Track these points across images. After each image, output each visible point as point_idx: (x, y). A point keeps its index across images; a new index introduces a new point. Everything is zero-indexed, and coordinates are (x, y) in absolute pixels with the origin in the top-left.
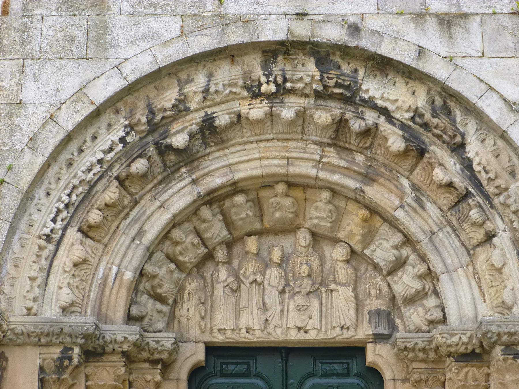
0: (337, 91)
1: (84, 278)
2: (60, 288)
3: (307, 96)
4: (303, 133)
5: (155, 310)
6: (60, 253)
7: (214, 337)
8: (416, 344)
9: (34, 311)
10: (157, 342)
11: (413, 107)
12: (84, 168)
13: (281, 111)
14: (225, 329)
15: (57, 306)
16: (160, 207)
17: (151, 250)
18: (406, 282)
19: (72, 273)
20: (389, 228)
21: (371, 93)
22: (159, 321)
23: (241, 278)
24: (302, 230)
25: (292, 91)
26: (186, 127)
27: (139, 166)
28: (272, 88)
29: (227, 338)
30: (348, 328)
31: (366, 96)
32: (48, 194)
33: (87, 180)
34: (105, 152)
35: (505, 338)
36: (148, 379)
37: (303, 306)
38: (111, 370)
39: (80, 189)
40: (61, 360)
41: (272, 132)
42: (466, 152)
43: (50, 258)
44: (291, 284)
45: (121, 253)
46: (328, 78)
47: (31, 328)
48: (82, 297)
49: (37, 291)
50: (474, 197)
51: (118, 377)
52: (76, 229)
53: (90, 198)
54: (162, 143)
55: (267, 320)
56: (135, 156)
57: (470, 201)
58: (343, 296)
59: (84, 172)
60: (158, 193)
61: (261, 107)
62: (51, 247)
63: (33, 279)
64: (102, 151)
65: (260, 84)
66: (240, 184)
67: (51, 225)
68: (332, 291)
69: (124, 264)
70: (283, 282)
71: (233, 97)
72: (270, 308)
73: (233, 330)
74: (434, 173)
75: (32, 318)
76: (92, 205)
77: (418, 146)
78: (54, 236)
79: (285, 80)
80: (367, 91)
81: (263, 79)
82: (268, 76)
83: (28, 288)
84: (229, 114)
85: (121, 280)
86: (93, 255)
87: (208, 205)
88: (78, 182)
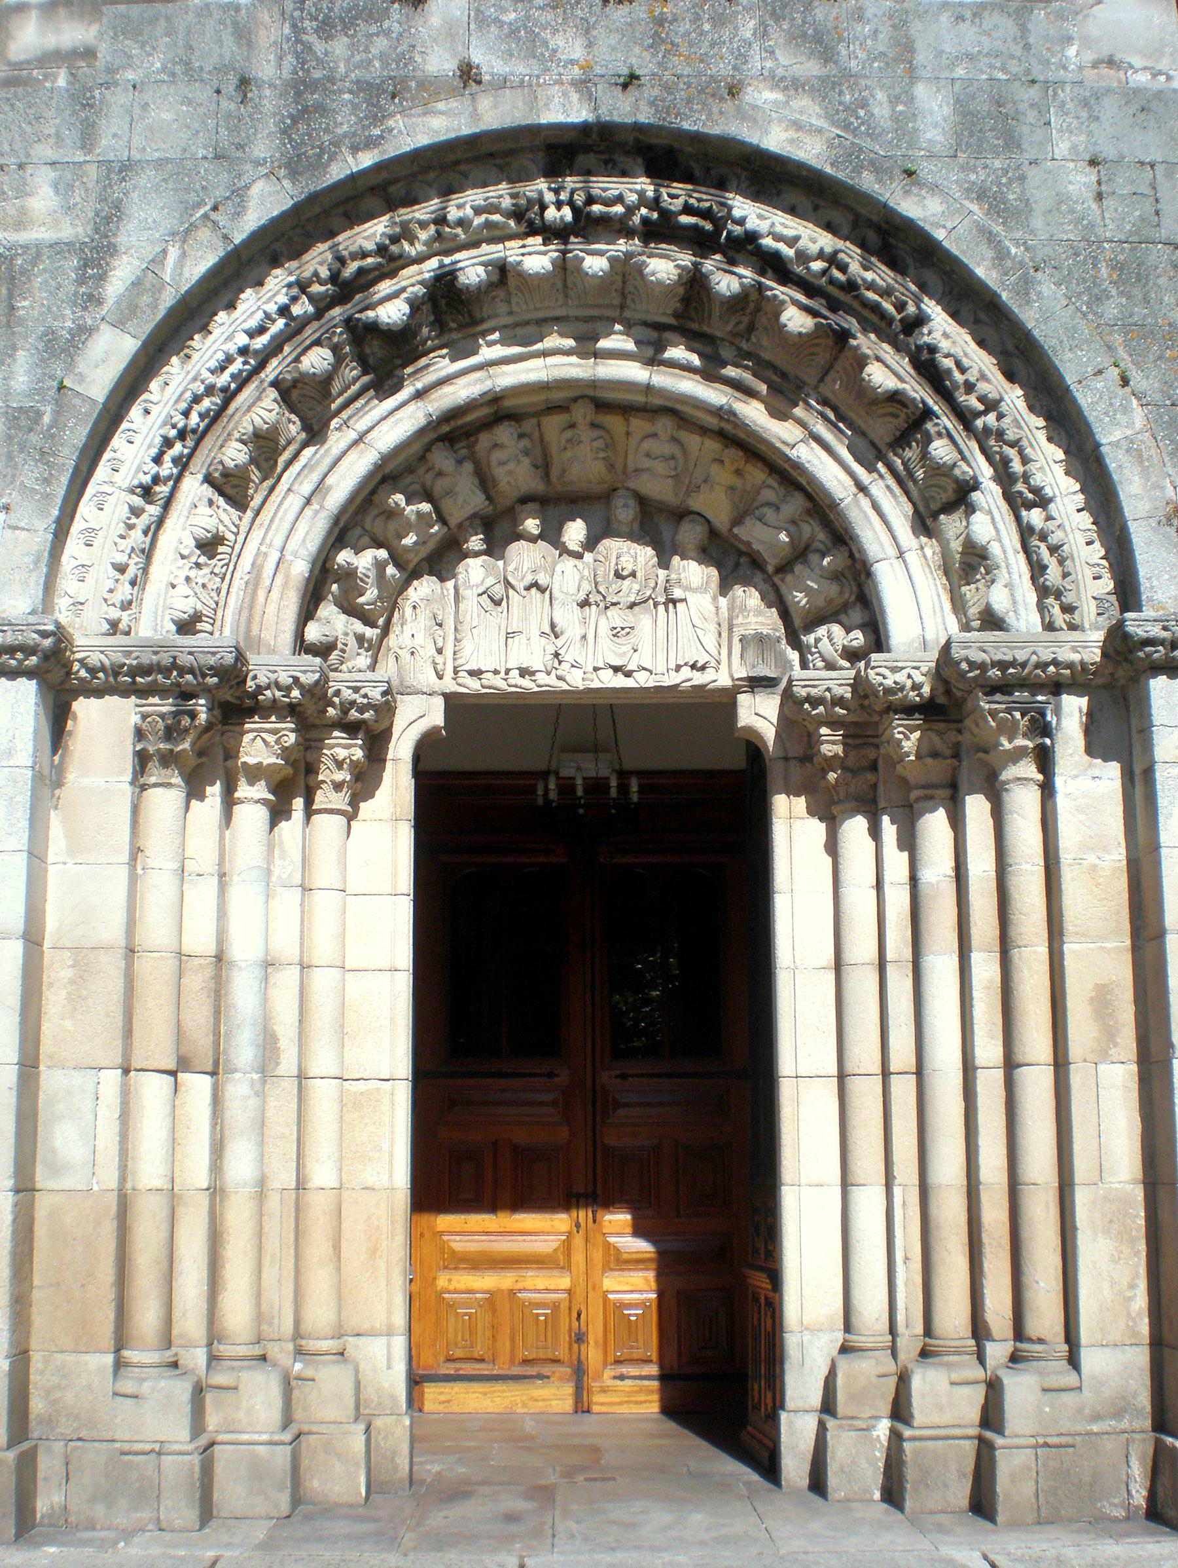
0: (685, 219)
1: (217, 570)
2: (174, 586)
3: (629, 233)
4: (623, 307)
5: (351, 634)
6: (169, 523)
7: (460, 685)
8: (828, 690)
9: (122, 626)
10: (356, 690)
11: (828, 250)
12: (213, 364)
13: (583, 259)
14: (482, 672)
15: (168, 617)
16: (355, 443)
17: (342, 524)
19: (193, 559)
20: (780, 484)
21: (752, 223)
22: (358, 654)
23: (510, 579)
24: (620, 492)
25: (604, 221)
26: (403, 290)
27: (317, 360)
28: (567, 213)
29: (483, 687)
30: (703, 668)
31: (738, 230)
32: (147, 412)
33: (219, 385)
34: (252, 334)
35: (994, 673)
36: (341, 758)
37: (623, 629)
38: (271, 739)
39: (206, 403)
40: (175, 714)
41: (566, 304)
42: (923, 334)
43: (153, 527)
44: (601, 589)
45: (287, 526)
46: (669, 195)
47: (118, 658)
48: (214, 606)
49: (125, 591)
50: (938, 418)
51: (286, 752)
52: (200, 477)
53: (225, 420)
54: (359, 320)
55: (557, 655)
56: (308, 342)
57: (929, 426)
59: (212, 372)
60: (354, 415)
61: (545, 253)
62: (153, 510)
63: (121, 569)
64: (246, 332)
65: (543, 207)
66: (507, 403)
67: (155, 469)
68: (674, 602)
69: (291, 547)
70: (587, 587)
72: (562, 633)
73: (496, 672)
74: (864, 375)
75: (119, 639)
76: (229, 435)
77: (837, 324)
78: (157, 489)
79: (590, 200)
80: (741, 222)
81: (549, 197)
82: (557, 192)
83: (110, 584)
84: (482, 264)
85: (287, 577)
86: (235, 530)
87: (447, 444)
88: (202, 388)
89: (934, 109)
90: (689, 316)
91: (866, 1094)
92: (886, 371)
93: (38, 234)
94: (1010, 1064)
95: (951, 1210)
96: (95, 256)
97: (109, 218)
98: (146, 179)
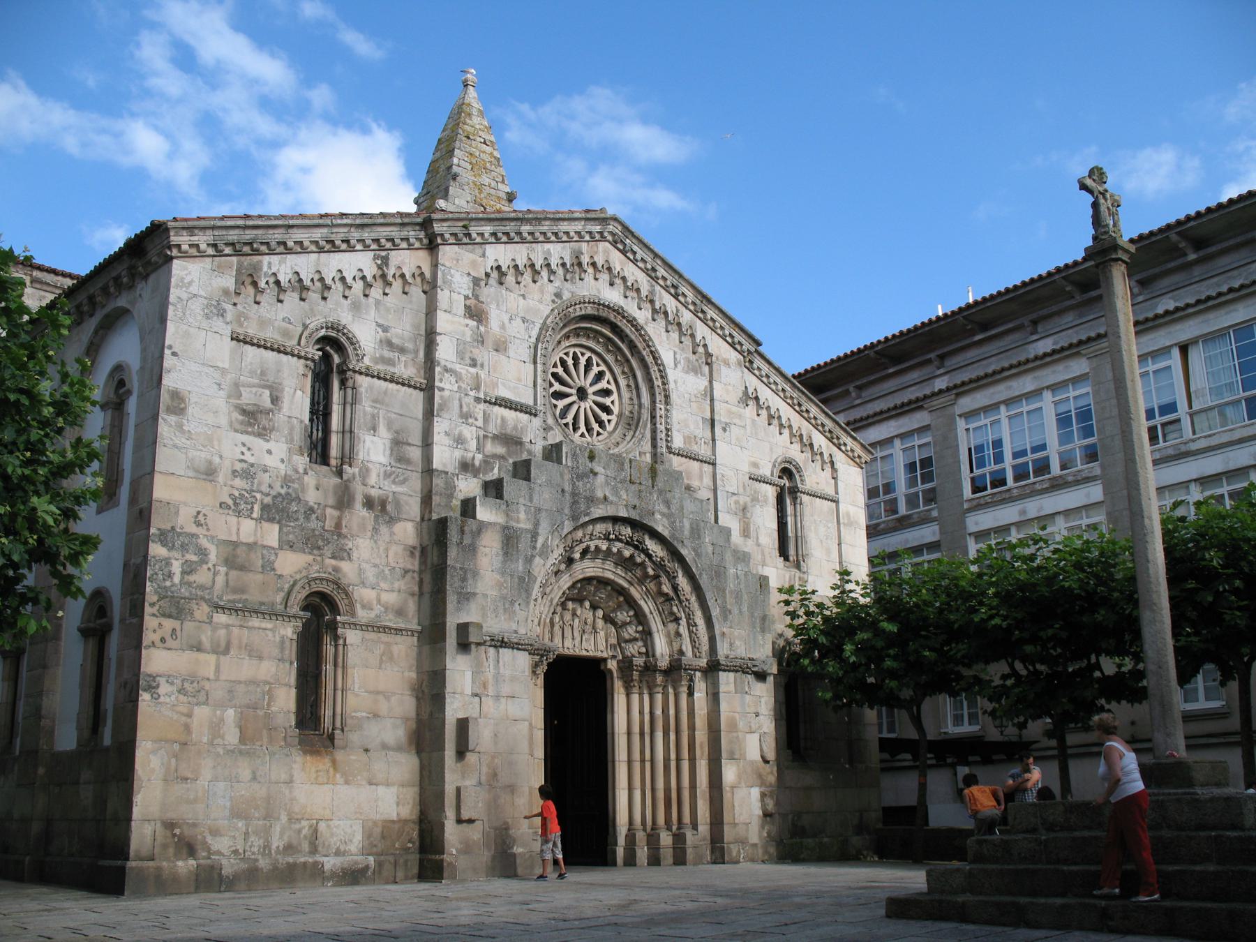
18: (631, 631)
58: (602, 634)
71: (600, 538)
89: (687, 524)
90: (627, 564)
91: (637, 767)
92: (666, 588)
93: (521, 525)
94: (678, 759)
95: (661, 795)
96: (534, 535)
97: (537, 525)
98: (544, 514)
